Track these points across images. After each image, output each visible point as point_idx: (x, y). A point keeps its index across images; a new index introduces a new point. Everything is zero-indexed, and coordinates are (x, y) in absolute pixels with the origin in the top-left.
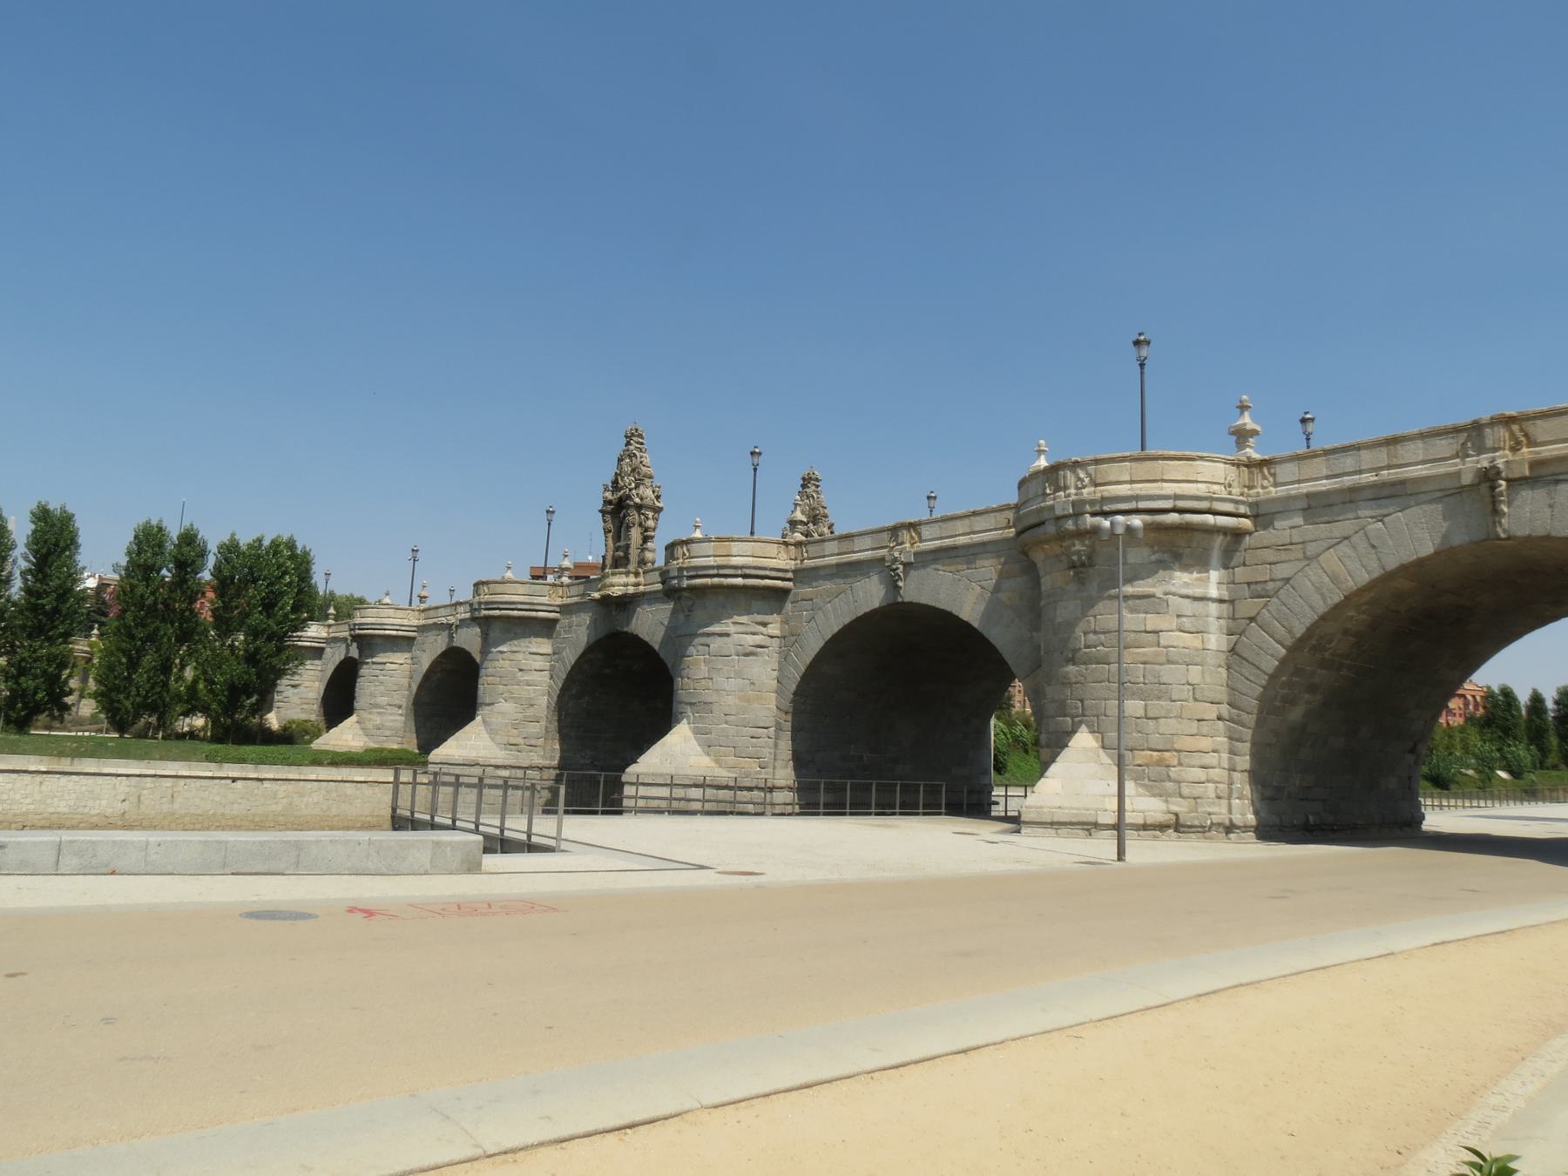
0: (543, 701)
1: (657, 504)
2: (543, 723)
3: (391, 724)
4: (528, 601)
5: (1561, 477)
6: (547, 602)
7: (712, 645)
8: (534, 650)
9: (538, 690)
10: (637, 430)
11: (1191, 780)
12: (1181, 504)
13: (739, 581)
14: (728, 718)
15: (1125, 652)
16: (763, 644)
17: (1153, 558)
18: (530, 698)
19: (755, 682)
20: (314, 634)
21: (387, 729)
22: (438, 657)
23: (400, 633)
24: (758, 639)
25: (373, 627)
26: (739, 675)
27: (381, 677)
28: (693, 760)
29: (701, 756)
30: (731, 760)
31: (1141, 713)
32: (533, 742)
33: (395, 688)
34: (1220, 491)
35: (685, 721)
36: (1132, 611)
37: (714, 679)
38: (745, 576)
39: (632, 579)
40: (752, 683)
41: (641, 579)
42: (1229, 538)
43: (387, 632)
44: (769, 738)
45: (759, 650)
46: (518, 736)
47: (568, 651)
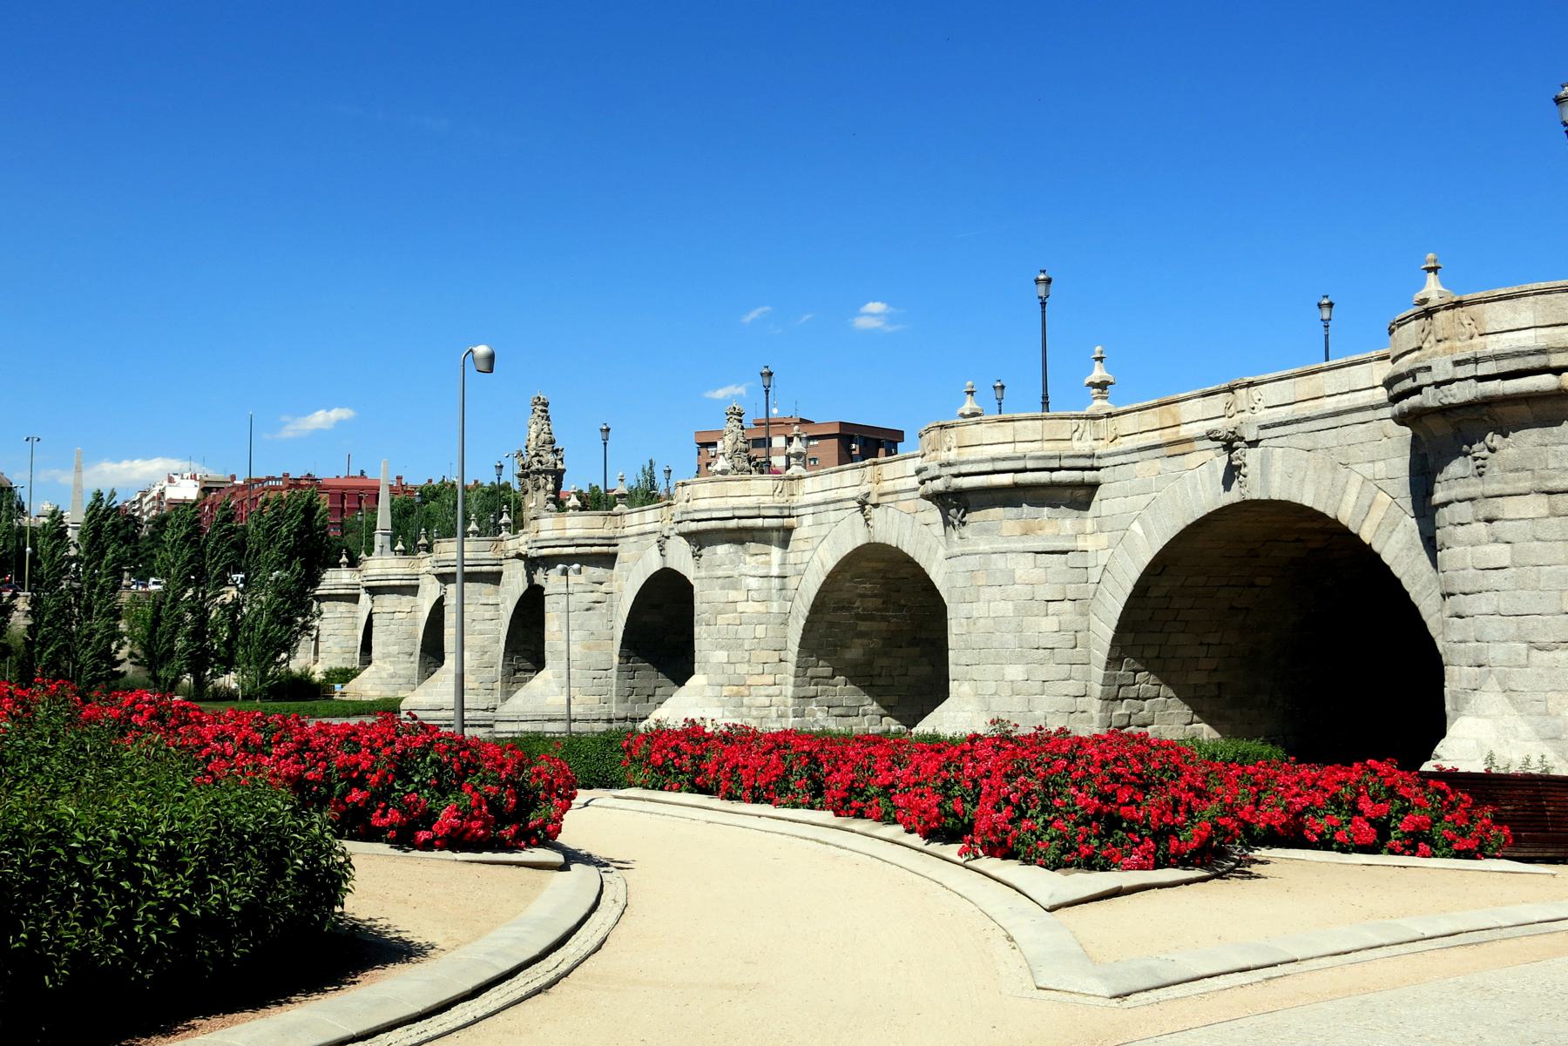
1: (560, 466)
4: (473, 557)
5: (889, 505)
6: (490, 557)
8: (485, 602)
10: (539, 398)
11: (758, 705)
12: (738, 513)
15: (719, 617)
17: (731, 550)
18: (485, 646)
20: (348, 581)
21: (400, 677)
23: (404, 583)
24: (595, 597)
25: (379, 578)
27: (392, 626)
31: (726, 660)
32: (490, 686)
34: (768, 501)
36: (722, 588)
38: (578, 546)
42: (782, 533)
43: (392, 583)
45: (596, 604)
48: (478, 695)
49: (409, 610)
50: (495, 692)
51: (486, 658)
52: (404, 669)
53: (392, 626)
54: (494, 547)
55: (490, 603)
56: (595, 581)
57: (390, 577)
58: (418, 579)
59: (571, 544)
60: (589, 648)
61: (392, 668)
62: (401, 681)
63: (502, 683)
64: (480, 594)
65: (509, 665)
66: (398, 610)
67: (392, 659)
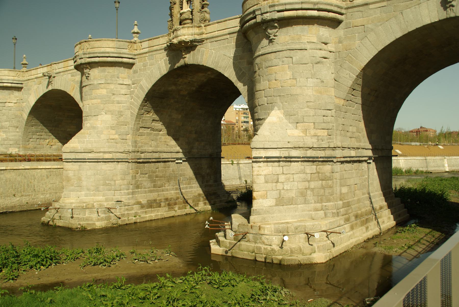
0: (128, 113)
2: (131, 126)
3: (12, 137)
4: (116, 51)
6: (128, 53)
7: (294, 58)
8: (121, 82)
9: (124, 106)
13: (315, 13)
14: (309, 104)
16: (326, 56)
18: (121, 111)
19: (325, 81)
22: (41, 97)
24: (323, 53)
26: (313, 76)
27: (4, 111)
28: (289, 132)
29: (293, 129)
30: (313, 132)
32: (124, 137)
33: (14, 117)
35: (276, 108)
37: (298, 79)
38: (319, 10)
39: (196, 30)
40: (322, 82)
41: (203, 30)
44: (332, 116)
46: (116, 134)
47: (144, 81)
48: (116, 143)
49: (16, 102)
50: (128, 141)
51: (122, 119)
52: (13, 136)
53: (4, 111)
54: (130, 47)
55: (125, 84)
56: (323, 41)
57: (3, 81)
58: (22, 84)
59: (316, 7)
60: (320, 93)
61: (4, 135)
62: (11, 142)
63: (133, 135)
64: (118, 78)
65: (138, 124)
66: (8, 101)
67: (4, 130)
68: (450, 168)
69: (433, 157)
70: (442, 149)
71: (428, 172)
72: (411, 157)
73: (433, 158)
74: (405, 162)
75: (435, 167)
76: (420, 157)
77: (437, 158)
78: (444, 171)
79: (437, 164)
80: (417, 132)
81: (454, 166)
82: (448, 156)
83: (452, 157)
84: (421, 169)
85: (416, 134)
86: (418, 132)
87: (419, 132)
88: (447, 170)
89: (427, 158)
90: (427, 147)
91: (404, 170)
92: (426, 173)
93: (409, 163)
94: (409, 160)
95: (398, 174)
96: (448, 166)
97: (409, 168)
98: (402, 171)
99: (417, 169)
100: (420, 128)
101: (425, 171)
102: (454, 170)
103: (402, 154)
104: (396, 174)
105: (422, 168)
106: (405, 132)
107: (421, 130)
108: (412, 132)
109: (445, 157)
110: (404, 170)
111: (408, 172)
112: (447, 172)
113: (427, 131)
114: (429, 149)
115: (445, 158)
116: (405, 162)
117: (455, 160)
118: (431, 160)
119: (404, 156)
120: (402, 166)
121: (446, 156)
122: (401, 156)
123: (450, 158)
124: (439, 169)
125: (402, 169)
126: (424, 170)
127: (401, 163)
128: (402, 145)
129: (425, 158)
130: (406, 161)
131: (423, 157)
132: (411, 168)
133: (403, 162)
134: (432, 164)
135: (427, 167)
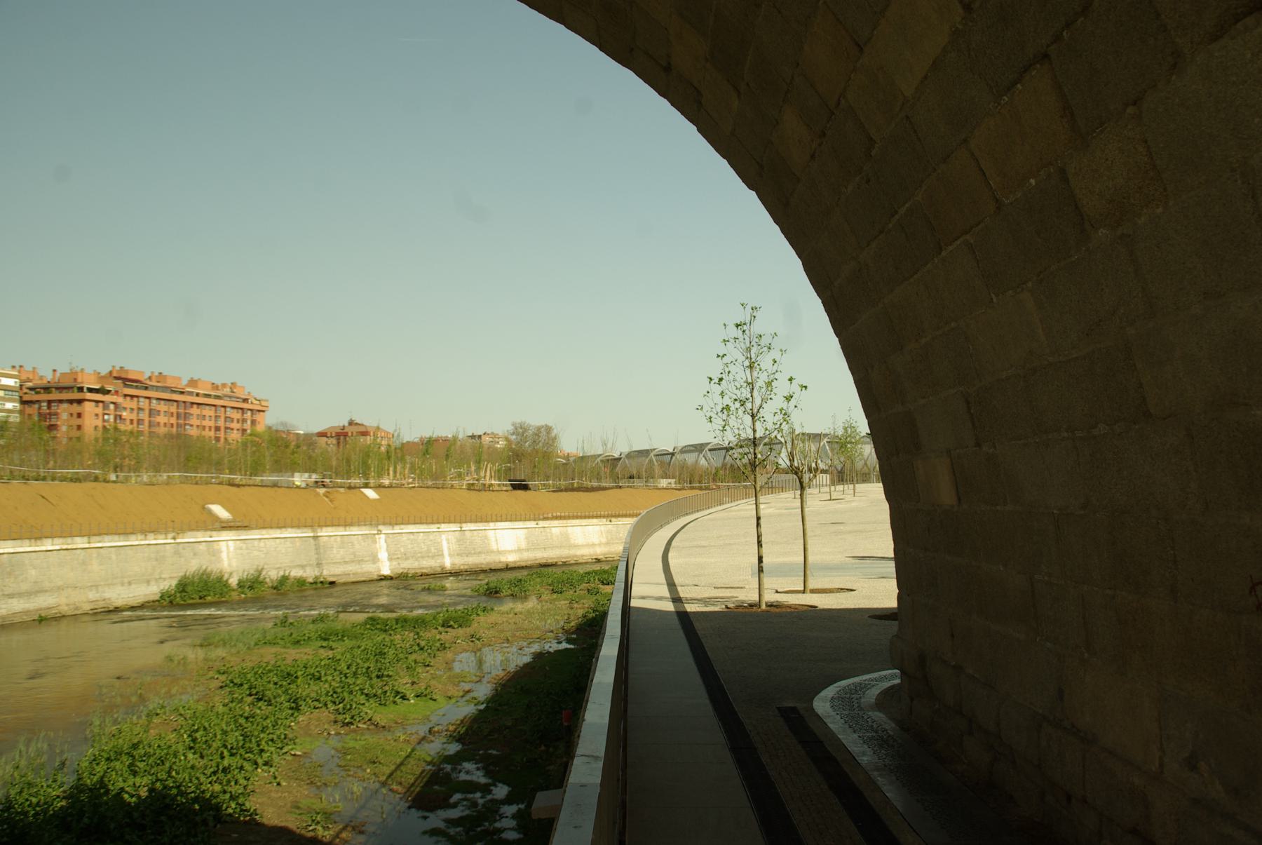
68: (395, 563)
69: (342, 528)
70: (375, 500)
71: (322, 582)
72: (264, 531)
73: (341, 531)
74: (241, 549)
75: (346, 563)
76: (294, 530)
77: (355, 531)
78: (375, 577)
79: (354, 554)
80: (338, 435)
81: (407, 559)
82: (392, 524)
83: (402, 526)
84: (296, 573)
85: (334, 441)
86: (341, 435)
87: (346, 435)
88: (386, 571)
89: (319, 534)
90: (326, 495)
91: (234, 582)
92: (314, 586)
93: (256, 553)
94: (256, 543)
95: (209, 598)
96: (390, 559)
97: (252, 572)
98: (226, 585)
99: (281, 573)
100: (346, 424)
101: (311, 580)
102: (405, 571)
103: (228, 521)
104: (201, 598)
105: (303, 567)
106: (306, 435)
107: (349, 430)
108: (322, 434)
109: (380, 527)
110: (234, 582)
111: (252, 584)
112: (384, 578)
113: (365, 434)
114: (331, 501)
115: (380, 532)
116: (241, 549)
117: (412, 537)
118: (333, 538)
119: (238, 528)
120: (230, 565)
121: (384, 524)
122: (226, 526)
123: (397, 529)
124: (359, 571)
125: (225, 578)
126: (310, 574)
127: (224, 556)
128: (238, 486)
129: (312, 535)
130: (244, 546)
131: (305, 530)
132: (260, 572)
133: (232, 549)
134: (337, 553)
135: (319, 565)
